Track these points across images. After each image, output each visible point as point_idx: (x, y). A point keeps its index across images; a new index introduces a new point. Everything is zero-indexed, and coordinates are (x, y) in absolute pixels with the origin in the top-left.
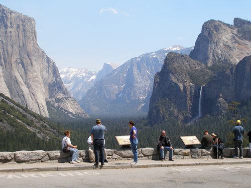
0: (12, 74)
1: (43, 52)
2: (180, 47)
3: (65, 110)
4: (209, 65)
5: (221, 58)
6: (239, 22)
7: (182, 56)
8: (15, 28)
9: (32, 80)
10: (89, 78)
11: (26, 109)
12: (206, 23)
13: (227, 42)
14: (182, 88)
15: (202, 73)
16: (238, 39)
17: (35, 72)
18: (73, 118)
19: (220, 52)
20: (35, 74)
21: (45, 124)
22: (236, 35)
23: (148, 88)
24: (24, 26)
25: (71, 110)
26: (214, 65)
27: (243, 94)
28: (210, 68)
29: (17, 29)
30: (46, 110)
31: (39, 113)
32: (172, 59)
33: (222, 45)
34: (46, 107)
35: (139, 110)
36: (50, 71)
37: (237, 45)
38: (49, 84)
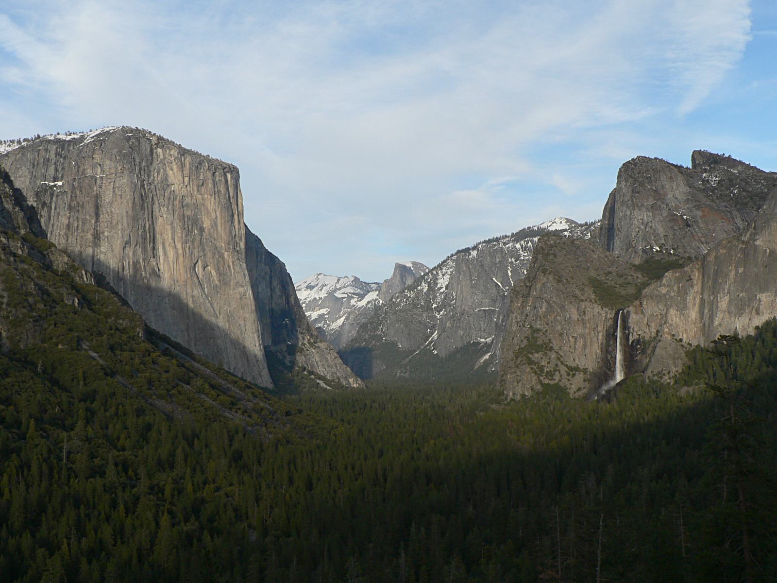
0: (189, 291)
1: (258, 241)
2: (568, 220)
3: (311, 373)
4: (637, 261)
5: (664, 244)
6: (705, 160)
7: (573, 242)
8: (195, 189)
9: (234, 305)
10: (361, 297)
11: (219, 370)
12: (626, 166)
13: (677, 208)
14: (575, 316)
15: (621, 281)
16: (704, 200)
17: (242, 286)
18: (326, 389)
19: (661, 231)
20: (241, 289)
21: (262, 404)
22: (699, 189)
23: (498, 318)
24: (214, 181)
25: (321, 371)
26: (647, 262)
27: (720, 325)
28: (638, 268)
29: (198, 190)
30: (265, 372)
31: (249, 379)
32: (552, 246)
33: (665, 213)
34: (265, 365)
35: (476, 367)
36: (275, 283)
37: (700, 213)
38: (272, 311)
